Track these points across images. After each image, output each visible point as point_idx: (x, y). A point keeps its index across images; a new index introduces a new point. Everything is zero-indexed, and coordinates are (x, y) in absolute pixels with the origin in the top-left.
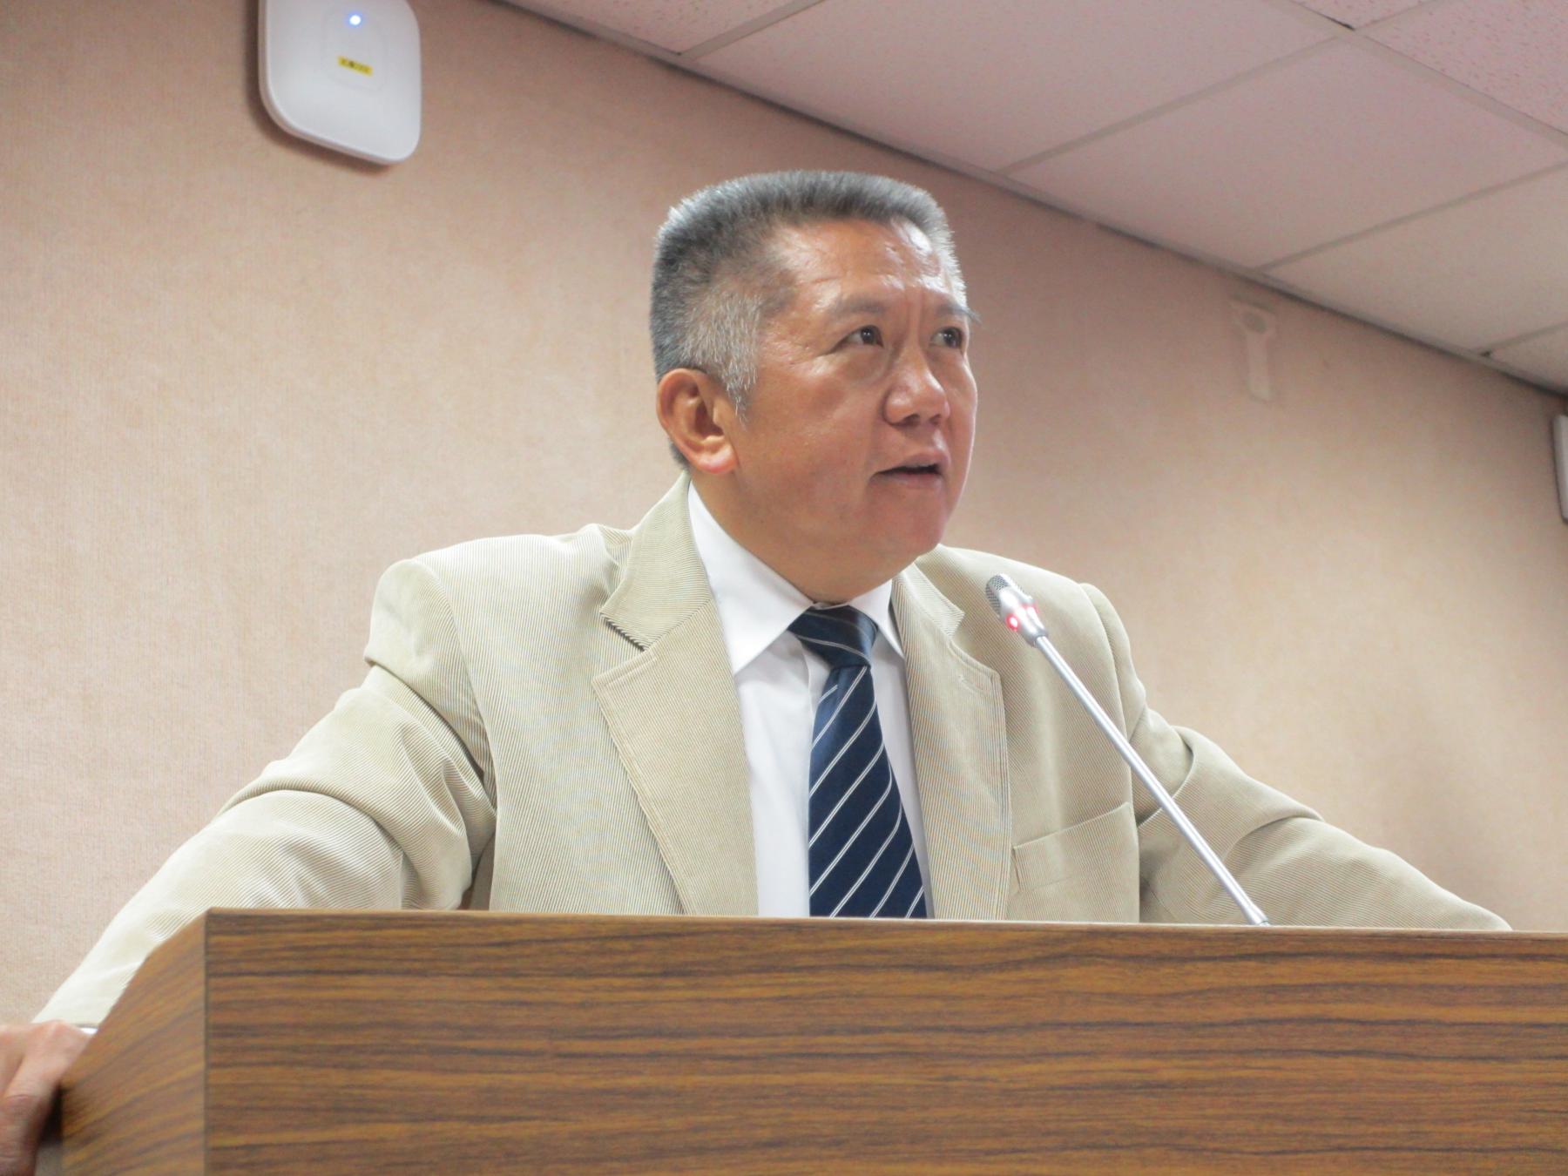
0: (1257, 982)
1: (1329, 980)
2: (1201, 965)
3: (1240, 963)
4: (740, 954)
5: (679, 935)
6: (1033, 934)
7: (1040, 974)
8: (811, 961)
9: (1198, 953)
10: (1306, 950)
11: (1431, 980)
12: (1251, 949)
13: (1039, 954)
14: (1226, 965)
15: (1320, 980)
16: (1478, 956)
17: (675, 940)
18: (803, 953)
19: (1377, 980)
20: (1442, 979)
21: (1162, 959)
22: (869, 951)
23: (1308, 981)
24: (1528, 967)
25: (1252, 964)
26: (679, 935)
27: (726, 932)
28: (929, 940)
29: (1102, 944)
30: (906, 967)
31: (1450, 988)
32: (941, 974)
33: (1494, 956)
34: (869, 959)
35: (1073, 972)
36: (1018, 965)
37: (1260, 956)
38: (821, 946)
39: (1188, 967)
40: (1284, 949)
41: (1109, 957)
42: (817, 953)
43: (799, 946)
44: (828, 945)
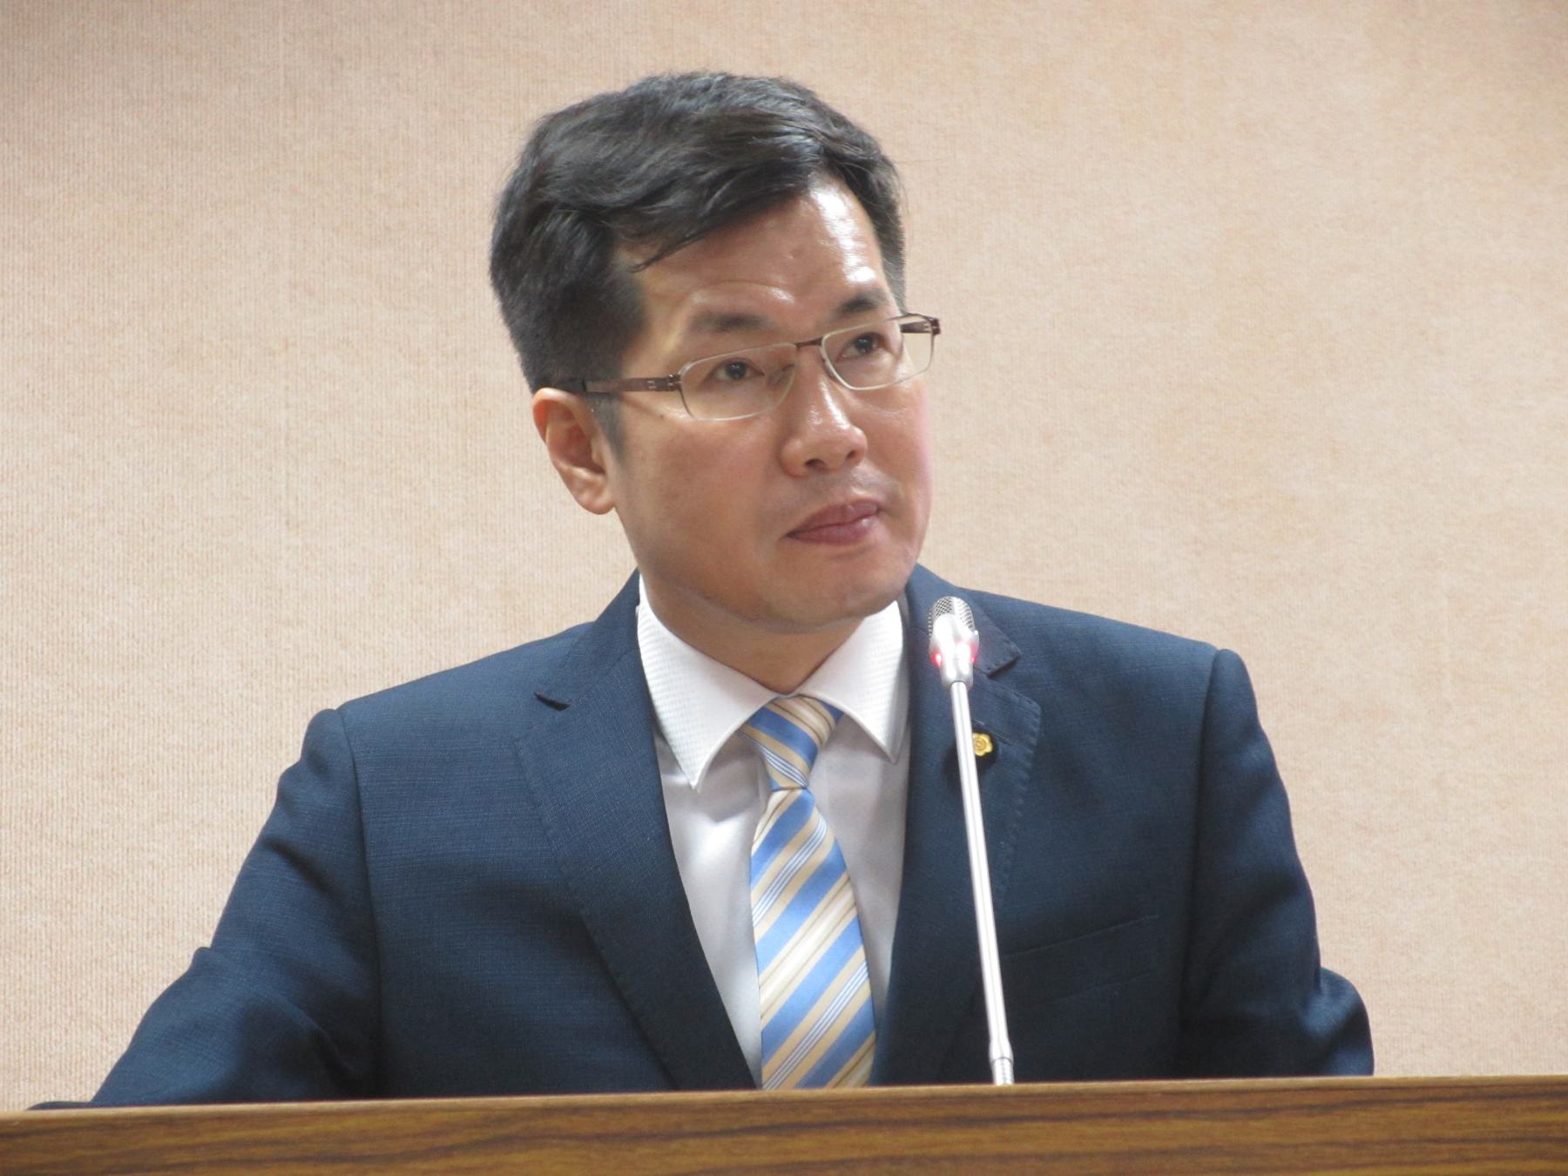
0: (765, 1159)
1: (866, 1154)
2: (692, 1143)
3: (750, 1138)
4: (100, 1152)
5: (25, 1135)
6: (469, 1114)
7: (476, 1161)
8: (187, 1157)
9: (687, 1128)
10: (838, 1118)
11: (1009, 1148)
12: (761, 1120)
13: (475, 1137)
14: (727, 1141)
15: (855, 1154)
16: (1080, 1117)
17: (20, 1141)
18: (179, 1148)
19: (936, 1151)
20: (1028, 1147)
21: (637, 1137)
22: (257, 1143)
23: (835, 1155)
24: (1158, 1127)
25: (763, 1138)
26: (25, 1135)
27: (80, 1128)
28: (335, 1127)
29: (557, 1122)
30: (302, 1160)
31: (1040, 1157)
32: (345, 1166)
33: (1105, 1116)
34: (261, 1152)
35: (519, 1158)
36: (448, 1152)
37: (774, 1129)
38: (198, 1140)
39: (675, 1145)
40: (806, 1118)
41: (569, 1137)
42: (192, 1148)
43: (171, 1141)
44: (207, 1138)
